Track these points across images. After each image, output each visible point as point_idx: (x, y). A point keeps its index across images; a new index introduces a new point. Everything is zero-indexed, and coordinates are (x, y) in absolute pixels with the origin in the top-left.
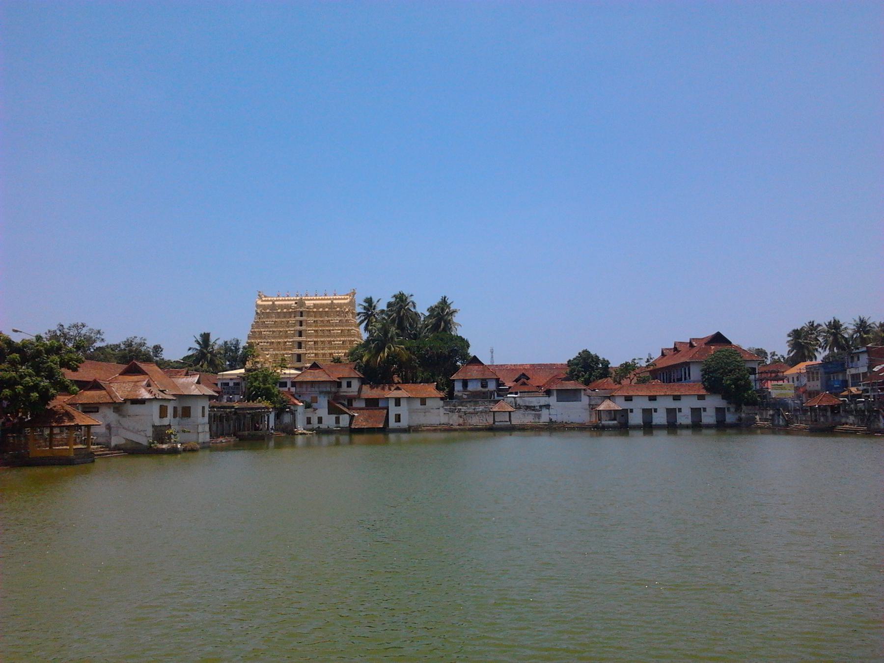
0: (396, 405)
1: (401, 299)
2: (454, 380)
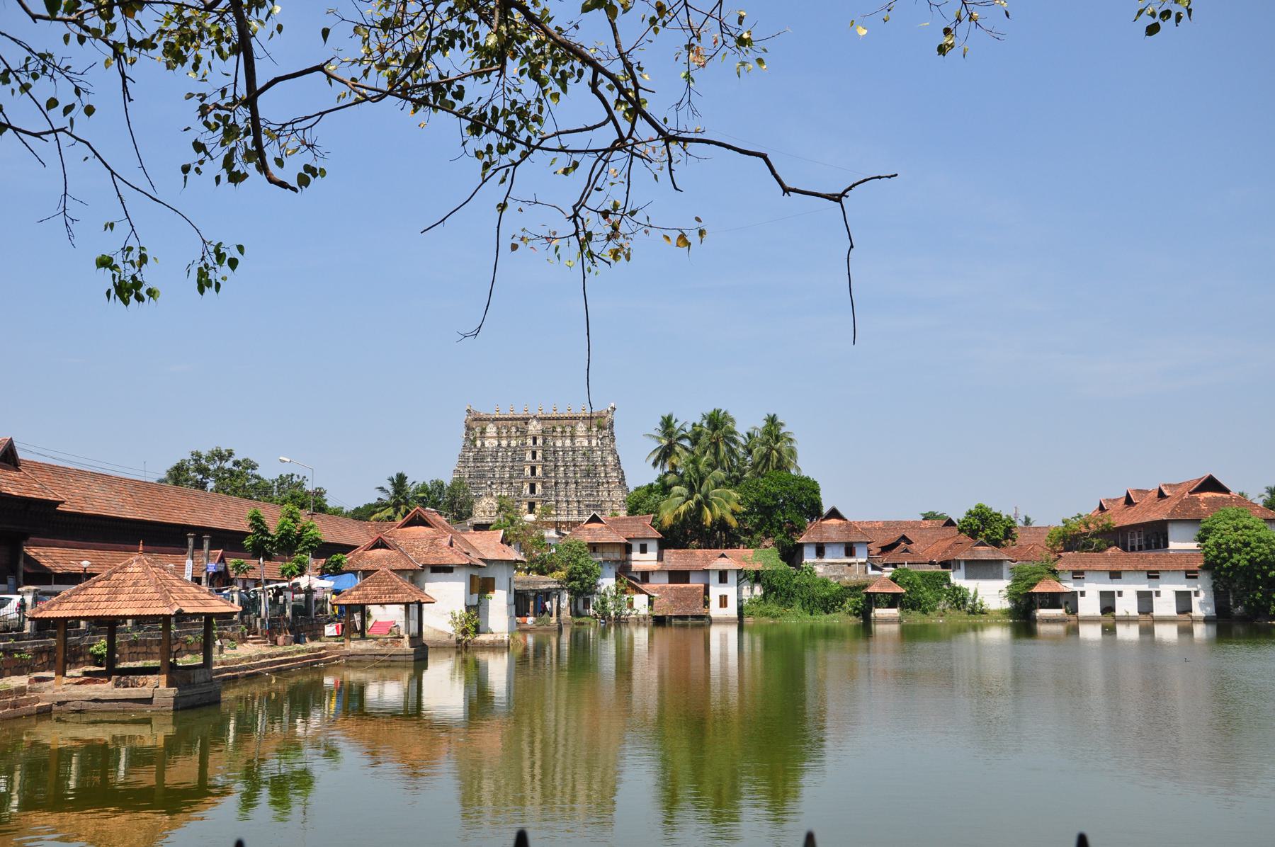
0: (721, 581)
1: (716, 421)
2: (801, 546)
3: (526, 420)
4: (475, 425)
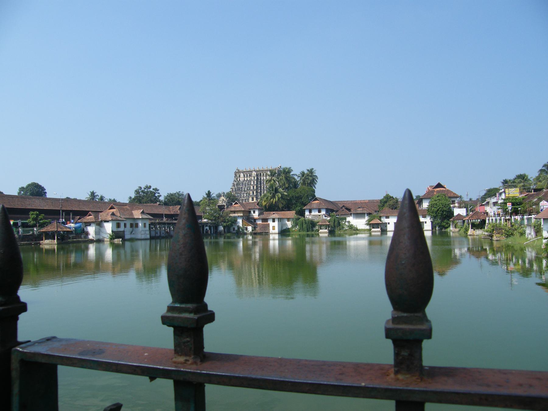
3: (252, 171)
4: (237, 173)
